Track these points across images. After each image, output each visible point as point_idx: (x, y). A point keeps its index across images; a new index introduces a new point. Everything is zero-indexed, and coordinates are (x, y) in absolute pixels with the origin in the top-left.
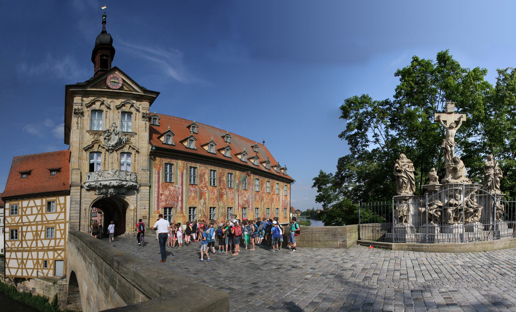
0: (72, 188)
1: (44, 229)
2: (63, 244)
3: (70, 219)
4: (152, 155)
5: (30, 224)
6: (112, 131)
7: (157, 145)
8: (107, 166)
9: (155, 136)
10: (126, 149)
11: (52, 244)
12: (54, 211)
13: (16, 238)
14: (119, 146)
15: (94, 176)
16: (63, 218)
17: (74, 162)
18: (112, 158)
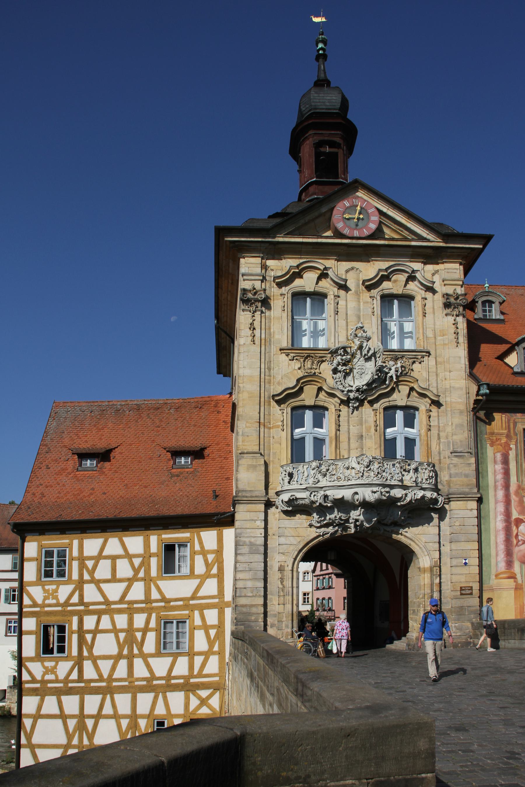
0: (240, 508)
1: (153, 624)
2: (216, 670)
3: (235, 597)
4: (481, 409)
5: (107, 608)
6: (355, 348)
7: (495, 381)
8: (344, 445)
9: (487, 351)
10: (399, 398)
11: (182, 667)
12: (185, 570)
13: (61, 650)
14: (378, 387)
15: (306, 474)
16: (215, 592)
17: (245, 436)
18: (361, 423)
